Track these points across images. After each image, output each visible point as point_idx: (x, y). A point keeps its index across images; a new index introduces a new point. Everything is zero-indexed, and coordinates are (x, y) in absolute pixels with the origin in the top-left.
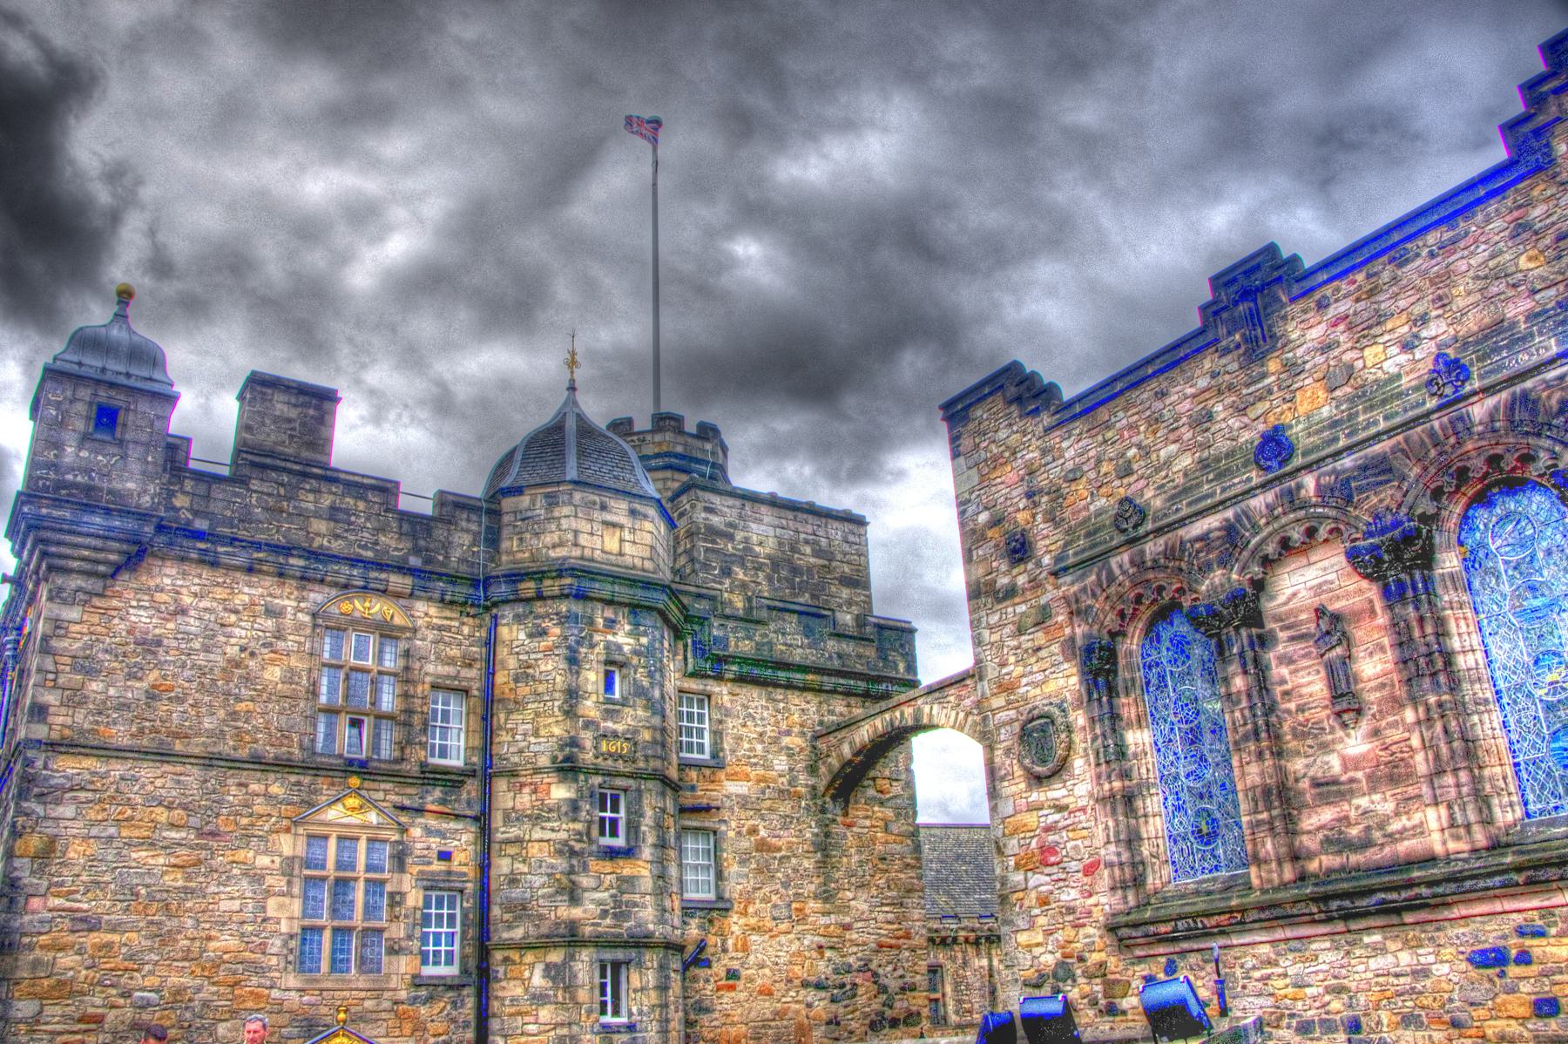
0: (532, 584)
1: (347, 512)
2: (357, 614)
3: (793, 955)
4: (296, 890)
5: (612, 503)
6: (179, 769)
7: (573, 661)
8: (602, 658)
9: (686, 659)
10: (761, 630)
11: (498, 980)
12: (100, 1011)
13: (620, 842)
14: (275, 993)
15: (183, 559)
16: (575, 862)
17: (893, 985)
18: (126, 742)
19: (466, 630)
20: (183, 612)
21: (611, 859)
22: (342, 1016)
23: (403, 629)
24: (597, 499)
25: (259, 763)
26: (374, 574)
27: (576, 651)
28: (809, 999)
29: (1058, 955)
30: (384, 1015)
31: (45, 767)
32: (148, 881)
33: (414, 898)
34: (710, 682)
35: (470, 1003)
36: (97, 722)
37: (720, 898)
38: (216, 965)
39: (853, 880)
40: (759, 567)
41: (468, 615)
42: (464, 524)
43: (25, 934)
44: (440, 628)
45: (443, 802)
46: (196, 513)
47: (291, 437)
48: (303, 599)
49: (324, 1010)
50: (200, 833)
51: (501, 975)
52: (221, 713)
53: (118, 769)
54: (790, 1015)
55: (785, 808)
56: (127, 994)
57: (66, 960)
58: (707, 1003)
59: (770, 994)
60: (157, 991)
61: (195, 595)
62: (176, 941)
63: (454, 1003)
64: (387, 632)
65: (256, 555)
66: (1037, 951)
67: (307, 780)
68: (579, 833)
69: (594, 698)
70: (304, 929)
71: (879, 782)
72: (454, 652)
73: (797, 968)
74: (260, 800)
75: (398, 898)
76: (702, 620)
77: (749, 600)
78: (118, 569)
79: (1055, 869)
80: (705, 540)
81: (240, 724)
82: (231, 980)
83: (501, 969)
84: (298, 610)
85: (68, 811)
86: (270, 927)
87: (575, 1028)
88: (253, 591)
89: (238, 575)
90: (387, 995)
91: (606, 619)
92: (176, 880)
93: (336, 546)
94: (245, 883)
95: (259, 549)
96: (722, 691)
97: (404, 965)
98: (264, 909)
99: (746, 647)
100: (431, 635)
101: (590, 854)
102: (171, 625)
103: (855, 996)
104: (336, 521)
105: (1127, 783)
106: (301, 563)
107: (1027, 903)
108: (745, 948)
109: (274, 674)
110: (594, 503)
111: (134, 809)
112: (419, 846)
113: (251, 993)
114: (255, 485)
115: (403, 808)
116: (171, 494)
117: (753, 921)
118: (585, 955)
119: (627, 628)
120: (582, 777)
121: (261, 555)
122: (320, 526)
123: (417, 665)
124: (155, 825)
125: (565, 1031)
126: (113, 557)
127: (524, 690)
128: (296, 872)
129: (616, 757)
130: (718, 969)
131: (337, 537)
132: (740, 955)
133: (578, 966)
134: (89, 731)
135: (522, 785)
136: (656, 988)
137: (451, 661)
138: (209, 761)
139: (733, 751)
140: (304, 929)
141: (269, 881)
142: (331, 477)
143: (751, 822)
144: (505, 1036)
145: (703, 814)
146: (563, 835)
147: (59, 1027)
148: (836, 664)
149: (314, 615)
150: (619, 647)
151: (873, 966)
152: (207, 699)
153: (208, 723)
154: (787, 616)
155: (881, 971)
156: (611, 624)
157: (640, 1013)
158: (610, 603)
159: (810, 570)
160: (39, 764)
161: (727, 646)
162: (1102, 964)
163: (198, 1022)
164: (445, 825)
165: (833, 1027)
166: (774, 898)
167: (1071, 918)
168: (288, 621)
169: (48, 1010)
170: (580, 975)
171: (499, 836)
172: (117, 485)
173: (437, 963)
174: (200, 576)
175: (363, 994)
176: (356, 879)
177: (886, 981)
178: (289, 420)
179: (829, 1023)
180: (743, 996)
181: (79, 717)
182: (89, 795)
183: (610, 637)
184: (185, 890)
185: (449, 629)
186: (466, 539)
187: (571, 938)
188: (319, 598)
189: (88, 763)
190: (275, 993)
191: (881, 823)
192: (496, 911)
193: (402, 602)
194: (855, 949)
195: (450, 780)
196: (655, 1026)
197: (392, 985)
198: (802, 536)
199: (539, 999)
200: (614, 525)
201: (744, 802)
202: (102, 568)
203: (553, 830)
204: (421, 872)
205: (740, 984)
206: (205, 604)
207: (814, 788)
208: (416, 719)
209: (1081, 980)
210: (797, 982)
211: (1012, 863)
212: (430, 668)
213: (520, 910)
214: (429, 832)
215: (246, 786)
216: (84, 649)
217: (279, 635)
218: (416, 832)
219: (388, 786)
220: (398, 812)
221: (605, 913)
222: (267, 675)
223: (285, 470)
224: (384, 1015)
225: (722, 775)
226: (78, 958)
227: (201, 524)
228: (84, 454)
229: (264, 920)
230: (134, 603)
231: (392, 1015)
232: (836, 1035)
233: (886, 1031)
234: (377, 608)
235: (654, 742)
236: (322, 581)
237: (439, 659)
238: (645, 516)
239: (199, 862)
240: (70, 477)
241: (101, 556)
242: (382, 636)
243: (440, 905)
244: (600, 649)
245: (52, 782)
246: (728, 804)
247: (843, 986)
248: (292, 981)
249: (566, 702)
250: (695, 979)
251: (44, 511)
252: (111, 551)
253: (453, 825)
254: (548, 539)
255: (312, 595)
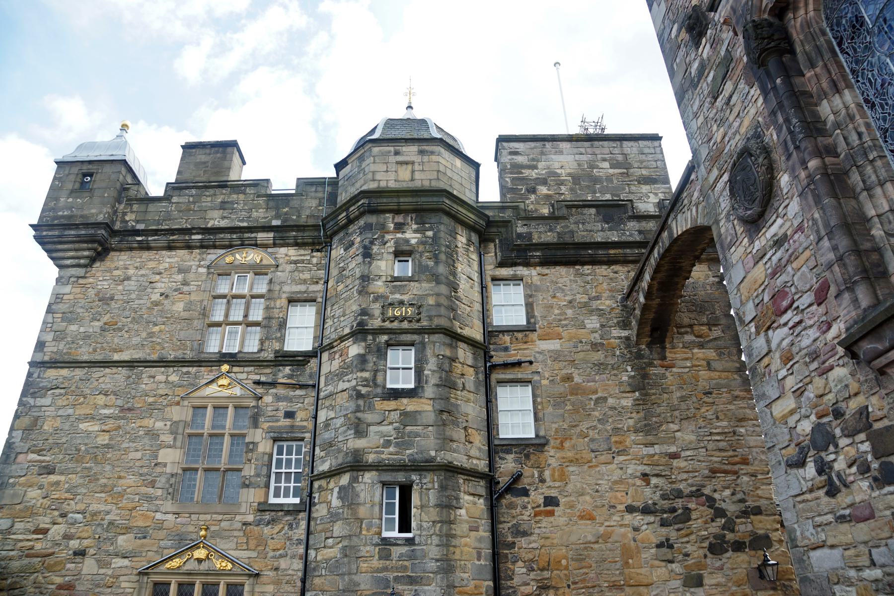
0: (344, 214)
1: (232, 203)
2: (237, 263)
3: (616, 482)
4: (179, 444)
5: (404, 149)
6: (114, 370)
7: (367, 254)
8: (392, 250)
9: (496, 255)
10: (563, 223)
11: (315, 505)
12: (47, 526)
13: (412, 386)
14: (159, 516)
15: (131, 249)
16: (361, 402)
17: (732, 508)
18: (85, 358)
19: (315, 260)
20: (128, 278)
21: (396, 398)
22: (203, 533)
23: (268, 266)
24: (392, 149)
25: (163, 363)
26: (246, 235)
27: (370, 248)
28: (636, 524)
29: (813, 418)
30: (236, 533)
31: (38, 377)
32: (86, 441)
33: (265, 446)
34: (521, 268)
35: (303, 524)
36: (71, 348)
37: (537, 436)
38: (121, 495)
39: (677, 413)
40: (562, 183)
41: (318, 251)
42: (313, 194)
43: (12, 477)
44: (295, 262)
45: (290, 377)
46: (137, 222)
47: (205, 171)
48: (203, 259)
49: (191, 528)
50: (122, 409)
51: (316, 501)
52: (144, 335)
53: (79, 373)
54: (614, 538)
55: (599, 356)
56: (64, 515)
57: (34, 494)
58: (524, 527)
59: (592, 518)
60: (82, 512)
61: (137, 268)
62: (98, 479)
63: (291, 527)
64: (259, 270)
65: (171, 238)
66: (792, 421)
67: (193, 370)
68: (366, 380)
69: (384, 279)
70: (185, 470)
71: (696, 328)
72: (306, 276)
73: (619, 495)
74: (161, 385)
75: (251, 446)
76: (506, 223)
77: (553, 206)
78: (93, 260)
79: (789, 314)
80: (511, 173)
81: (154, 339)
82: (130, 506)
83: (316, 495)
84: (199, 266)
85: (47, 401)
86: (158, 469)
87: (355, 539)
88: (171, 260)
89: (164, 252)
90: (238, 518)
91: (396, 224)
92: (104, 439)
93: (224, 224)
94: (146, 440)
95: (173, 234)
96: (532, 274)
97: (252, 496)
98: (156, 457)
99: (550, 237)
100: (290, 267)
101: (376, 396)
102: (120, 288)
103: (689, 519)
104: (224, 209)
105: (829, 160)
106: (200, 237)
107: (773, 368)
108: (563, 477)
109: (179, 307)
110: (390, 152)
111: (85, 398)
112: (269, 409)
113: (142, 515)
114: (175, 199)
115: (258, 383)
116: (125, 214)
117: (570, 454)
118: (368, 477)
119: (415, 226)
120: (370, 337)
121: (174, 237)
122: (216, 214)
123: (277, 288)
124: (96, 406)
125: (345, 543)
126: (86, 253)
127: (341, 287)
128: (180, 431)
129: (403, 319)
130: (537, 497)
131: (223, 218)
132: (557, 484)
133: (359, 487)
134: (65, 354)
135: (335, 352)
136: (437, 506)
137: (305, 282)
138: (131, 364)
139: (544, 317)
140: (185, 470)
141: (162, 438)
142: (223, 185)
143: (564, 372)
144: (316, 549)
145: (517, 369)
146: (354, 383)
147: (20, 537)
148: (638, 238)
149: (208, 267)
150: (407, 241)
151: (707, 491)
152: (136, 327)
153: (136, 340)
154: (587, 211)
155: (716, 496)
156: (399, 227)
157: (420, 527)
158: (397, 212)
159: (609, 178)
160: (35, 375)
161: (530, 239)
162: (863, 411)
163: (105, 535)
164: (292, 393)
165: (665, 550)
166: (591, 433)
167: (815, 365)
168: (191, 276)
169: (18, 526)
170: (362, 495)
171: (322, 394)
172: (86, 212)
173: (286, 495)
174: (141, 257)
175: (220, 517)
176: (223, 435)
177: (723, 506)
178: (205, 163)
179: (660, 546)
180: (562, 521)
181: (61, 347)
182: (62, 391)
183: (399, 235)
184: (107, 446)
185: (303, 261)
186: (314, 203)
187: (356, 465)
188: (213, 257)
189: (65, 372)
190: (159, 516)
191: (704, 363)
192: (317, 449)
193: (270, 250)
194: (685, 476)
195: (299, 360)
196: (435, 540)
197: (243, 510)
198: (599, 156)
199: (334, 517)
200: (407, 163)
201: (556, 356)
202: (82, 261)
203: (348, 381)
204: (270, 427)
205: (558, 511)
206: (142, 272)
207: (627, 338)
208: (274, 323)
209: (843, 442)
210: (622, 507)
211: (753, 330)
212: (286, 288)
213: (329, 445)
214: (278, 398)
215: (154, 377)
216: (69, 308)
217: (185, 283)
218: (268, 399)
219: (251, 369)
220: (255, 386)
221: (387, 444)
222: (175, 308)
223: (193, 187)
224: (236, 533)
225: (534, 336)
226: (39, 491)
227: (141, 227)
228: (70, 200)
229: (156, 465)
230: (101, 279)
231: (241, 534)
232: (670, 557)
233: (728, 555)
234: (252, 256)
235: (438, 305)
236: (215, 247)
237: (295, 282)
238: (432, 153)
239: (119, 427)
240: (60, 213)
241: (80, 254)
242: (256, 274)
243: (289, 453)
244: (391, 247)
245: (41, 385)
246: (540, 358)
247: (673, 510)
248: (169, 506)
249: (360, 284)
250: (511, 506)
251: (45, 233)
252: (84, 250)
253: (299, 392)
254: (358, 185)
255: (209, 256)
